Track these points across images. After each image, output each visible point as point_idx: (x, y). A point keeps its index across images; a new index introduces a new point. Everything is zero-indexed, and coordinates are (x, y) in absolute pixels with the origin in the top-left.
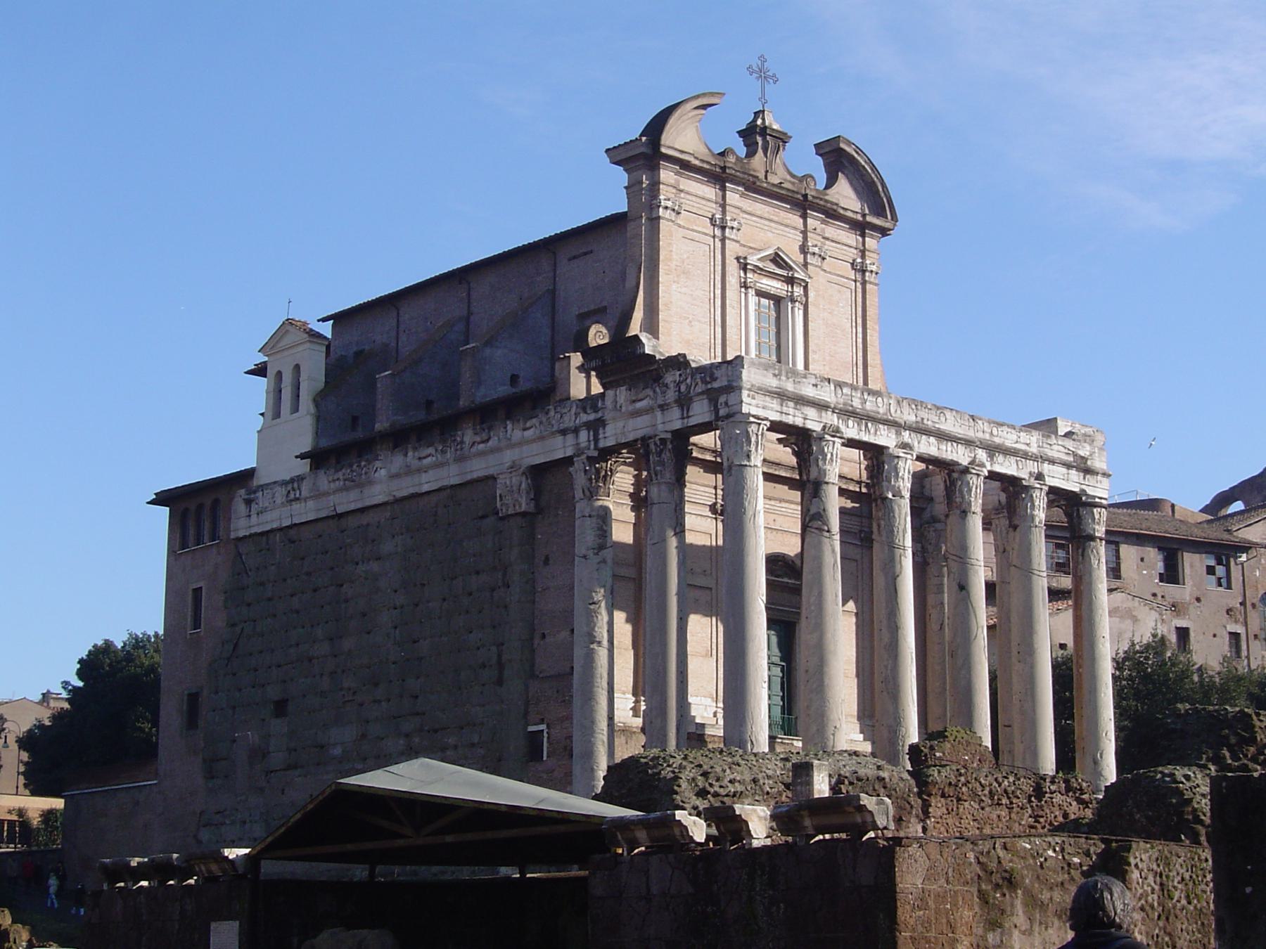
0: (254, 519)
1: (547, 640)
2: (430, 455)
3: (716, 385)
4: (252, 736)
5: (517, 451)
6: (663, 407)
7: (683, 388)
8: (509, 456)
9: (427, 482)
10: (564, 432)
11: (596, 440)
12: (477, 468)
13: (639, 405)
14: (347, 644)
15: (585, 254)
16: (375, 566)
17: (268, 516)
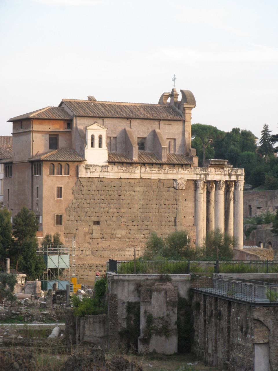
0: (89, 173)
1: (186, 218)
2: (155, 170)
3: (238, 173)
4: (86, 229)
5: (183, 175)
6: (224, 175)
7: (229, 172)
8: (180, 176)
9: (154, 176)
10: (197, 174)
11: (206, 178)
12: (170, 177)
13: (217, 173)
14: (123, 210)
15: (169, 124)
16: (133, 193)
17: (95, 174)
